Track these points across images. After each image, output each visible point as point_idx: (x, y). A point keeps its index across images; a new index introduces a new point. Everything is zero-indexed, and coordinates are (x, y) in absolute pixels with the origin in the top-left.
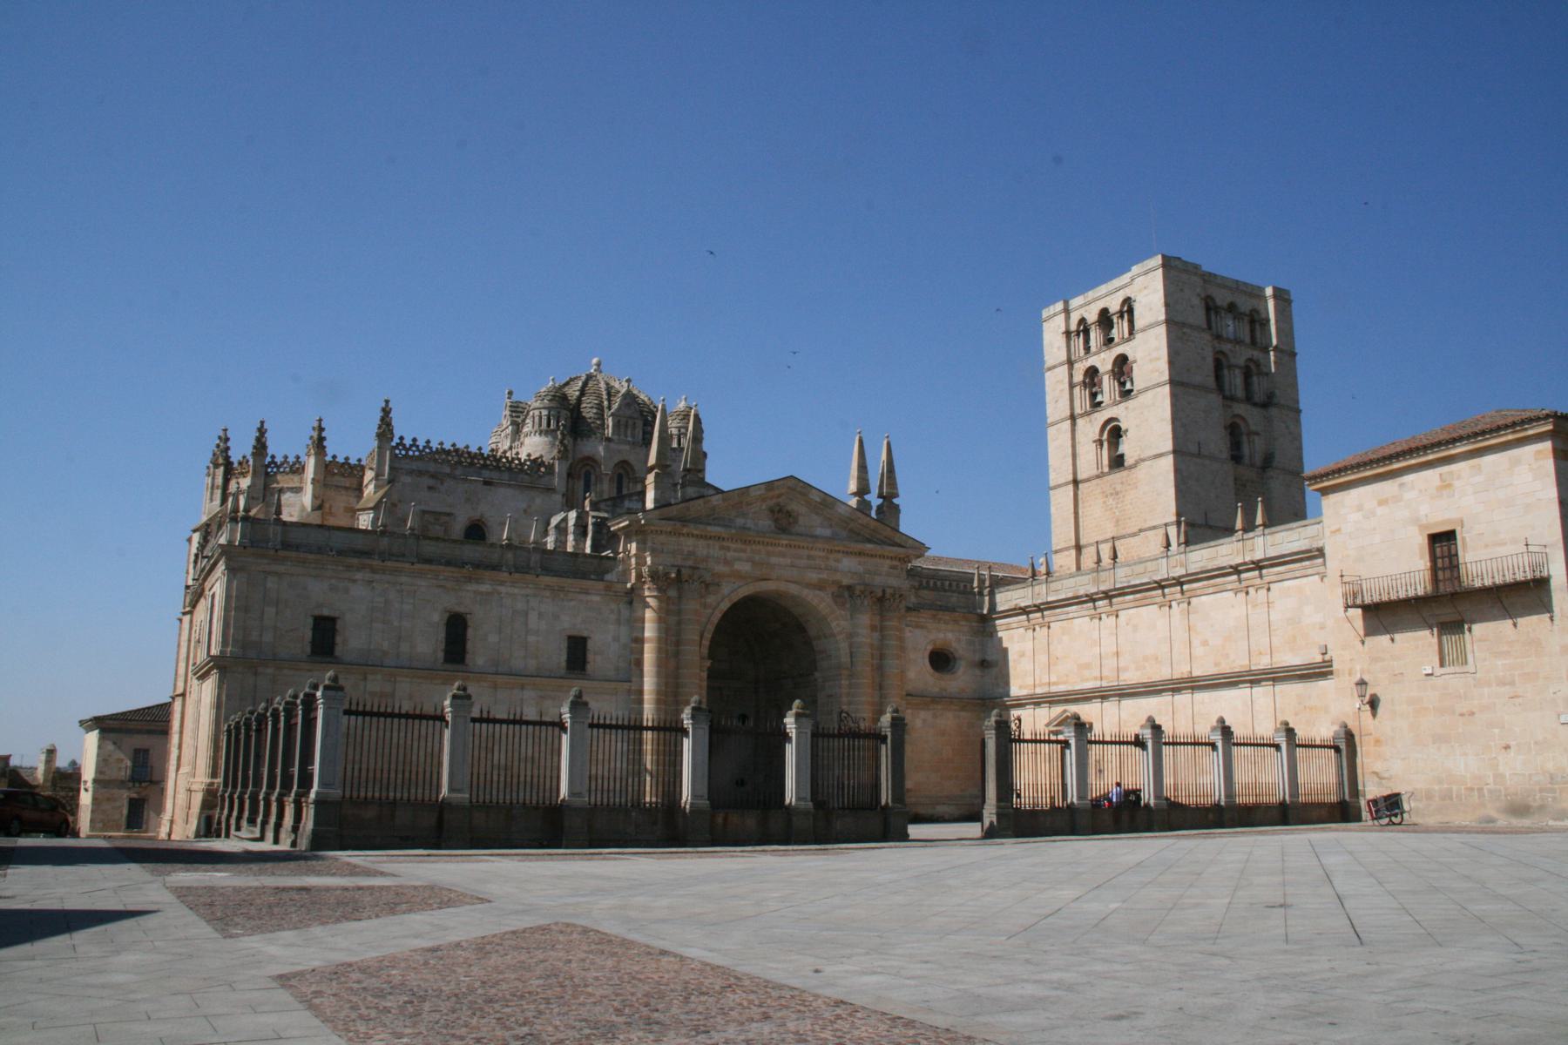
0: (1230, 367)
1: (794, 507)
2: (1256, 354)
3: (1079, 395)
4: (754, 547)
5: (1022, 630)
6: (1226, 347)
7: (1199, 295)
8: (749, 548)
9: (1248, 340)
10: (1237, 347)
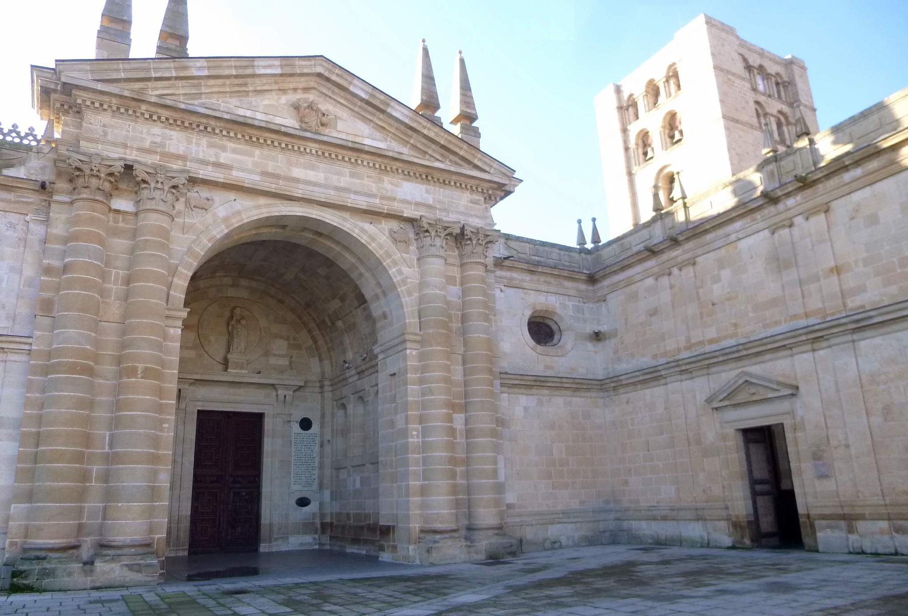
0: (766, 115)
1: (325, 106)
2: (785, 109)
3: (632, 155)
4: (266, 152)
5: (650, 281)
6: (762, 99)
7: (736, 51)
8: (257, 152)
9: (776, 96)
10: (769, 99)
